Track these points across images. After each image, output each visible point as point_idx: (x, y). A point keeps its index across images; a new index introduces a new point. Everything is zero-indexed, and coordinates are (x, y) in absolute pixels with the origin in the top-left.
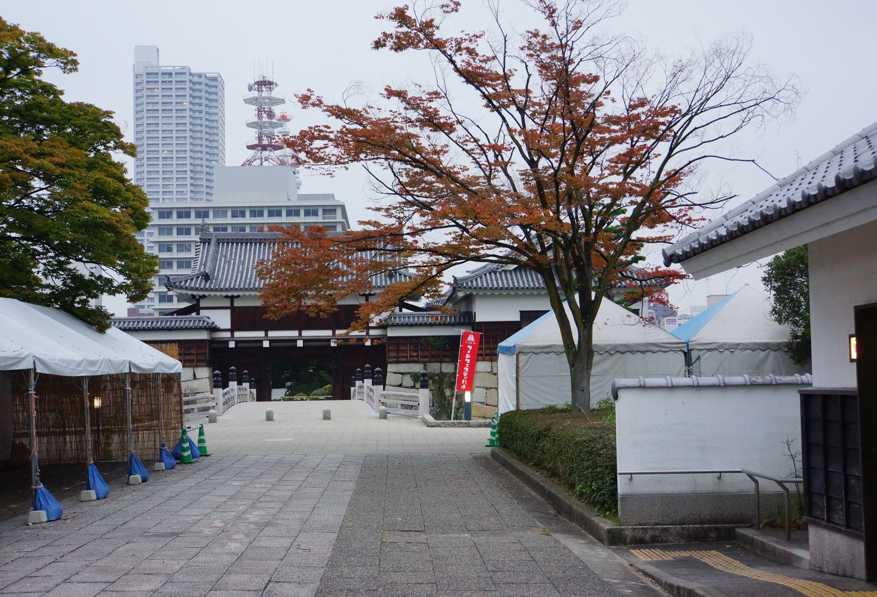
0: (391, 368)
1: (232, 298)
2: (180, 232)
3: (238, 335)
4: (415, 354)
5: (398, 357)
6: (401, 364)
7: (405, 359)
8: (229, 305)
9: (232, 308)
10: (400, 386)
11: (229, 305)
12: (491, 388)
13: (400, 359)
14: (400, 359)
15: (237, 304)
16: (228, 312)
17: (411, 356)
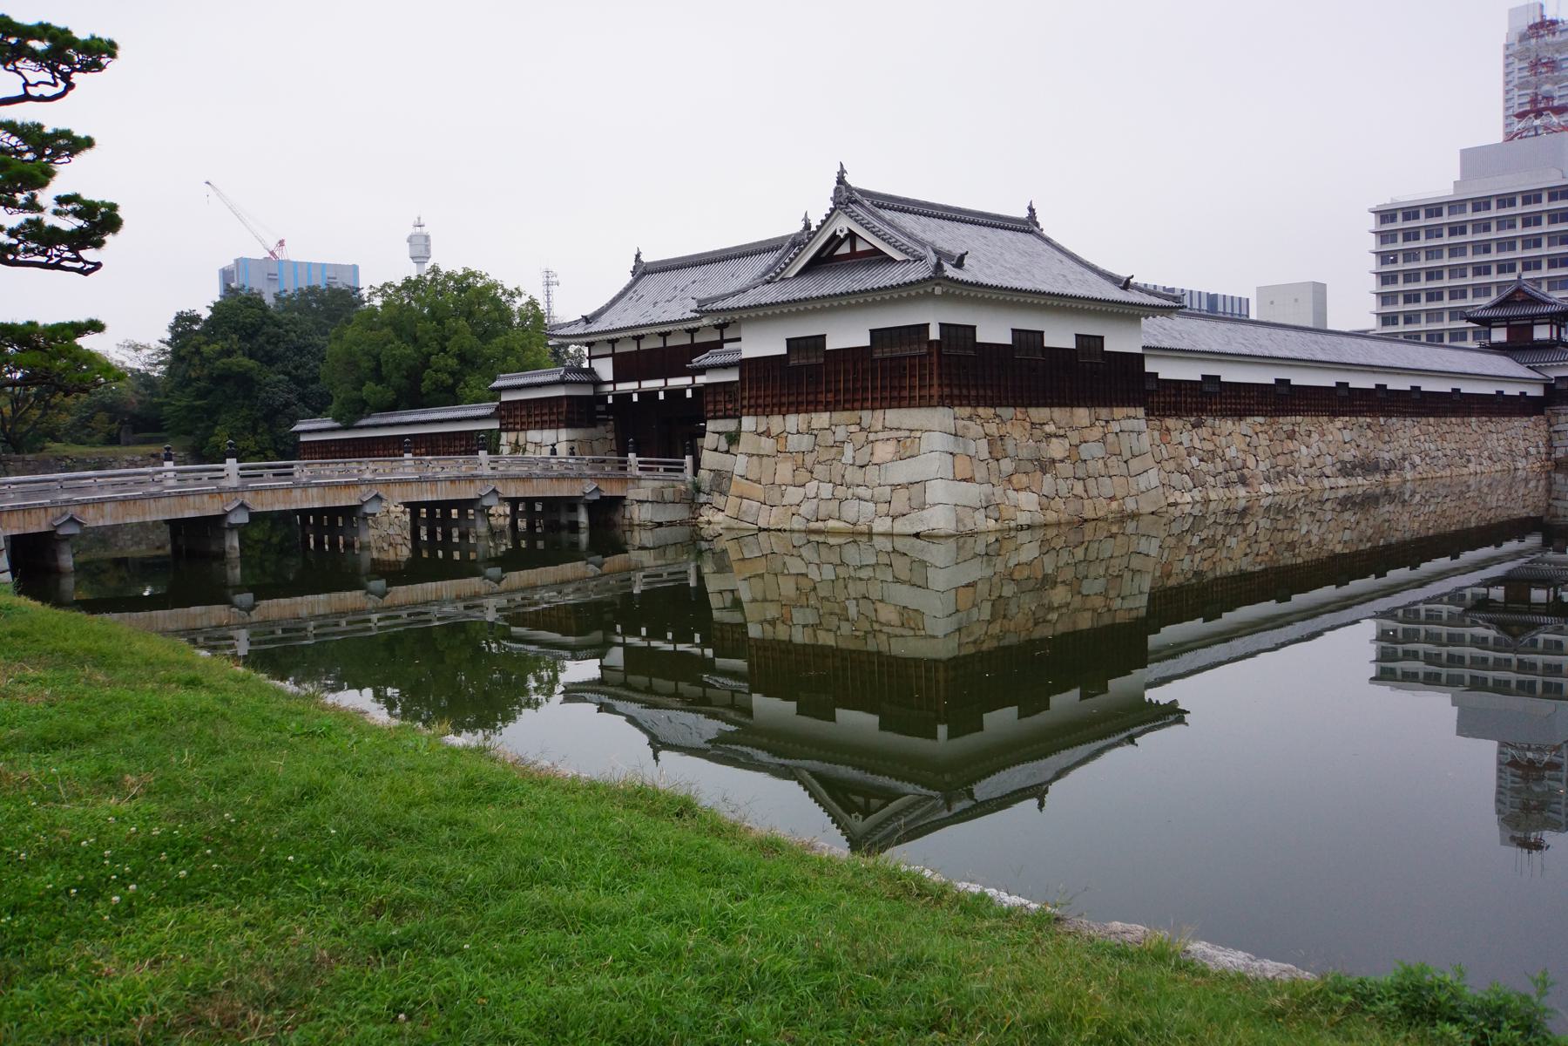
0: (711, 426)
1: (613, 342)
2: (1407, 238)
3: (623, 387)
4: (729, 407)
5: (715, 411)
6: (719, 421)
7: (721, 414)
8: (611, 352)
9: (613, 355)
10: (716, 450)
11: (611, 352)
12: (753, 455)
13: (718, 414)
14: (718, 414)
15: (619, 349)
16: (610, 360)
17: (726, 410)
